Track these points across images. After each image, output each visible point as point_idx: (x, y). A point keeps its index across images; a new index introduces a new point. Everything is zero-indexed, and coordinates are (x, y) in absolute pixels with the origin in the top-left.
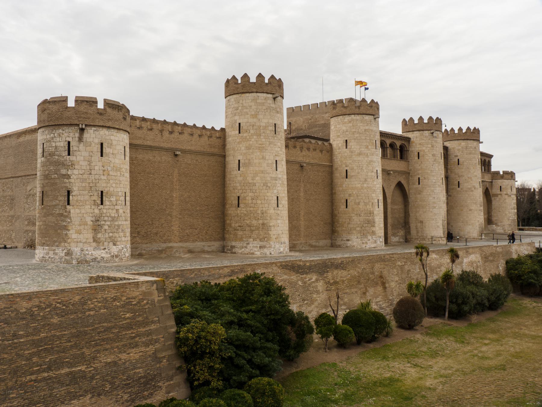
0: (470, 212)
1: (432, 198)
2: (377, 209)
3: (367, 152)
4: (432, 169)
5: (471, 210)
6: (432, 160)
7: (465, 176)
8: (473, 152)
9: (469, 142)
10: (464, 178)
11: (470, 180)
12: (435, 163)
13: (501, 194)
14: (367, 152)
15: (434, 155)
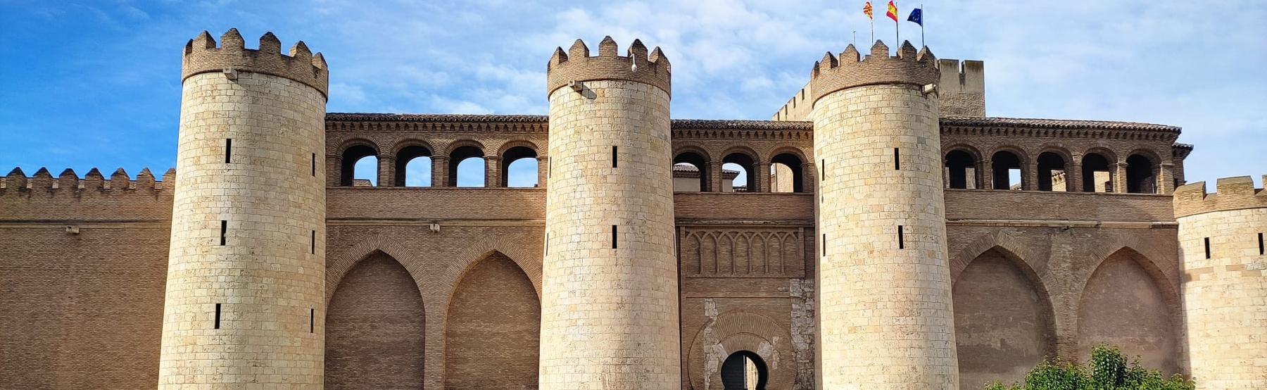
0: (852, 336)
1: (564, 294)
2: (214, 332)
3: (197, 174)
4: (574, 203)
5: (853, 329)
6: (575, 173)
7: (839, 213)
8: (867, 126)
9: (849, 94)
10: (834, 221)
11: (851, 225)
12: (583, 180)
13: (1209, 270)
14: (197, 174)
15: (579, 158)
